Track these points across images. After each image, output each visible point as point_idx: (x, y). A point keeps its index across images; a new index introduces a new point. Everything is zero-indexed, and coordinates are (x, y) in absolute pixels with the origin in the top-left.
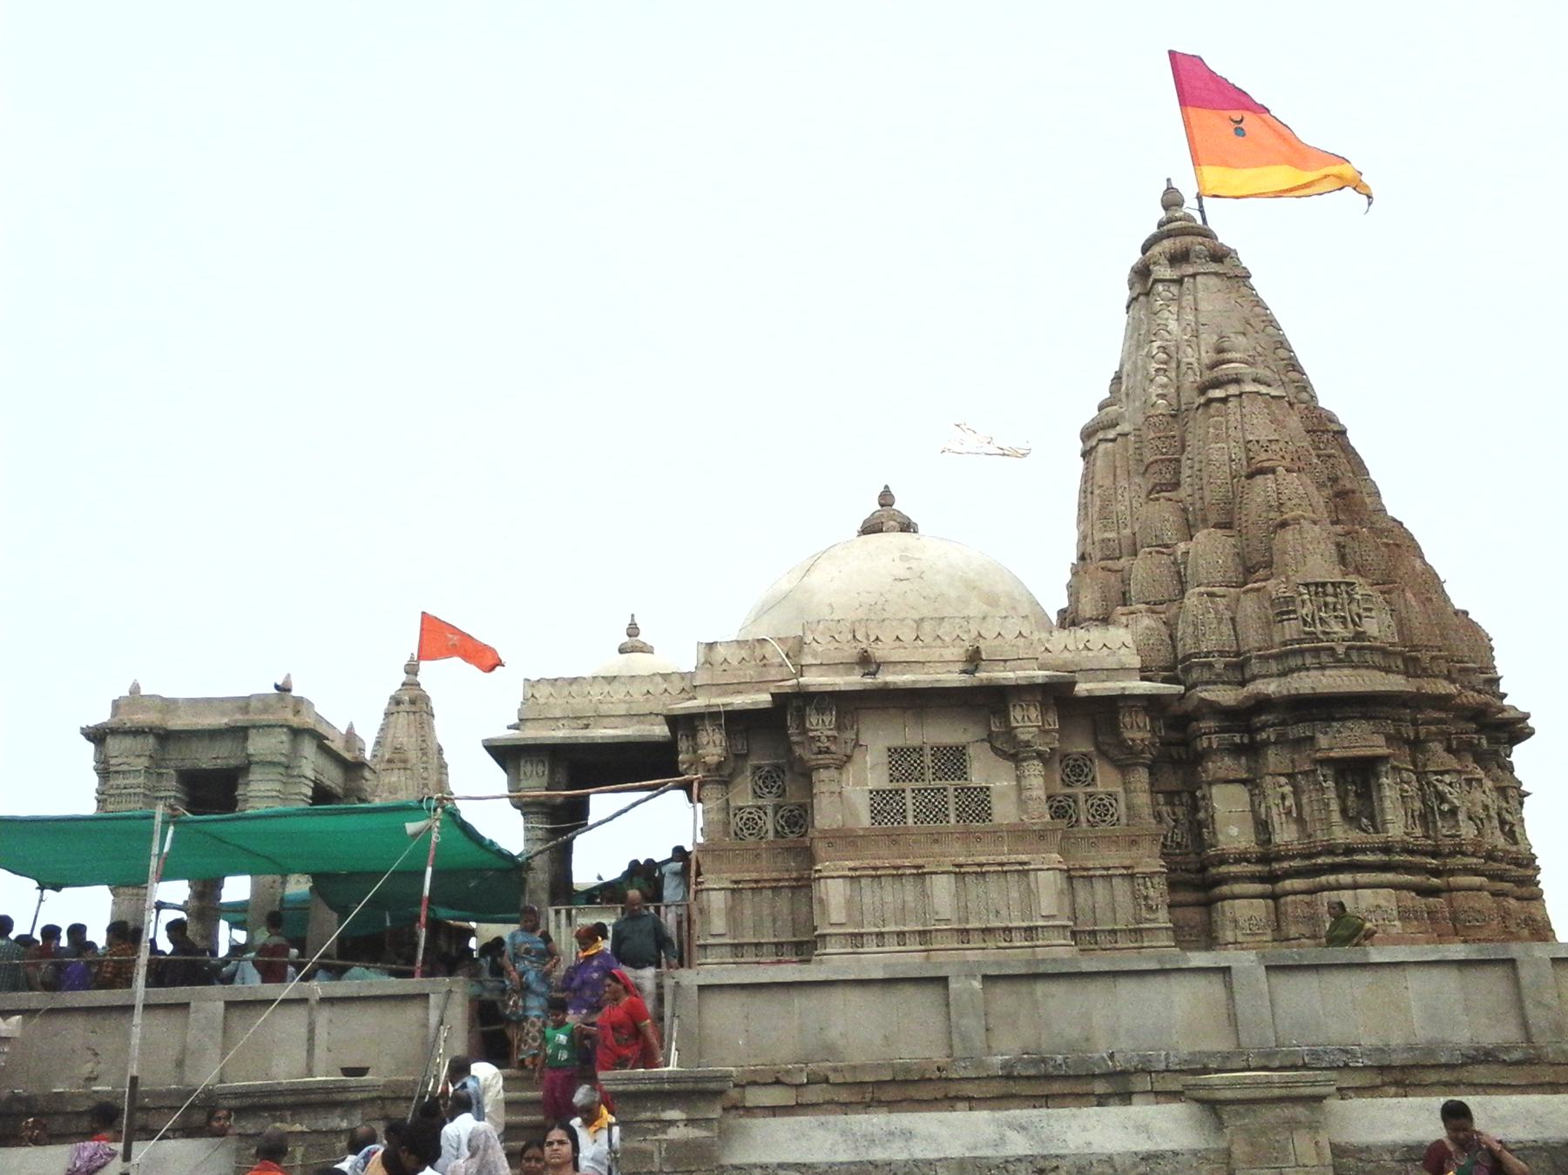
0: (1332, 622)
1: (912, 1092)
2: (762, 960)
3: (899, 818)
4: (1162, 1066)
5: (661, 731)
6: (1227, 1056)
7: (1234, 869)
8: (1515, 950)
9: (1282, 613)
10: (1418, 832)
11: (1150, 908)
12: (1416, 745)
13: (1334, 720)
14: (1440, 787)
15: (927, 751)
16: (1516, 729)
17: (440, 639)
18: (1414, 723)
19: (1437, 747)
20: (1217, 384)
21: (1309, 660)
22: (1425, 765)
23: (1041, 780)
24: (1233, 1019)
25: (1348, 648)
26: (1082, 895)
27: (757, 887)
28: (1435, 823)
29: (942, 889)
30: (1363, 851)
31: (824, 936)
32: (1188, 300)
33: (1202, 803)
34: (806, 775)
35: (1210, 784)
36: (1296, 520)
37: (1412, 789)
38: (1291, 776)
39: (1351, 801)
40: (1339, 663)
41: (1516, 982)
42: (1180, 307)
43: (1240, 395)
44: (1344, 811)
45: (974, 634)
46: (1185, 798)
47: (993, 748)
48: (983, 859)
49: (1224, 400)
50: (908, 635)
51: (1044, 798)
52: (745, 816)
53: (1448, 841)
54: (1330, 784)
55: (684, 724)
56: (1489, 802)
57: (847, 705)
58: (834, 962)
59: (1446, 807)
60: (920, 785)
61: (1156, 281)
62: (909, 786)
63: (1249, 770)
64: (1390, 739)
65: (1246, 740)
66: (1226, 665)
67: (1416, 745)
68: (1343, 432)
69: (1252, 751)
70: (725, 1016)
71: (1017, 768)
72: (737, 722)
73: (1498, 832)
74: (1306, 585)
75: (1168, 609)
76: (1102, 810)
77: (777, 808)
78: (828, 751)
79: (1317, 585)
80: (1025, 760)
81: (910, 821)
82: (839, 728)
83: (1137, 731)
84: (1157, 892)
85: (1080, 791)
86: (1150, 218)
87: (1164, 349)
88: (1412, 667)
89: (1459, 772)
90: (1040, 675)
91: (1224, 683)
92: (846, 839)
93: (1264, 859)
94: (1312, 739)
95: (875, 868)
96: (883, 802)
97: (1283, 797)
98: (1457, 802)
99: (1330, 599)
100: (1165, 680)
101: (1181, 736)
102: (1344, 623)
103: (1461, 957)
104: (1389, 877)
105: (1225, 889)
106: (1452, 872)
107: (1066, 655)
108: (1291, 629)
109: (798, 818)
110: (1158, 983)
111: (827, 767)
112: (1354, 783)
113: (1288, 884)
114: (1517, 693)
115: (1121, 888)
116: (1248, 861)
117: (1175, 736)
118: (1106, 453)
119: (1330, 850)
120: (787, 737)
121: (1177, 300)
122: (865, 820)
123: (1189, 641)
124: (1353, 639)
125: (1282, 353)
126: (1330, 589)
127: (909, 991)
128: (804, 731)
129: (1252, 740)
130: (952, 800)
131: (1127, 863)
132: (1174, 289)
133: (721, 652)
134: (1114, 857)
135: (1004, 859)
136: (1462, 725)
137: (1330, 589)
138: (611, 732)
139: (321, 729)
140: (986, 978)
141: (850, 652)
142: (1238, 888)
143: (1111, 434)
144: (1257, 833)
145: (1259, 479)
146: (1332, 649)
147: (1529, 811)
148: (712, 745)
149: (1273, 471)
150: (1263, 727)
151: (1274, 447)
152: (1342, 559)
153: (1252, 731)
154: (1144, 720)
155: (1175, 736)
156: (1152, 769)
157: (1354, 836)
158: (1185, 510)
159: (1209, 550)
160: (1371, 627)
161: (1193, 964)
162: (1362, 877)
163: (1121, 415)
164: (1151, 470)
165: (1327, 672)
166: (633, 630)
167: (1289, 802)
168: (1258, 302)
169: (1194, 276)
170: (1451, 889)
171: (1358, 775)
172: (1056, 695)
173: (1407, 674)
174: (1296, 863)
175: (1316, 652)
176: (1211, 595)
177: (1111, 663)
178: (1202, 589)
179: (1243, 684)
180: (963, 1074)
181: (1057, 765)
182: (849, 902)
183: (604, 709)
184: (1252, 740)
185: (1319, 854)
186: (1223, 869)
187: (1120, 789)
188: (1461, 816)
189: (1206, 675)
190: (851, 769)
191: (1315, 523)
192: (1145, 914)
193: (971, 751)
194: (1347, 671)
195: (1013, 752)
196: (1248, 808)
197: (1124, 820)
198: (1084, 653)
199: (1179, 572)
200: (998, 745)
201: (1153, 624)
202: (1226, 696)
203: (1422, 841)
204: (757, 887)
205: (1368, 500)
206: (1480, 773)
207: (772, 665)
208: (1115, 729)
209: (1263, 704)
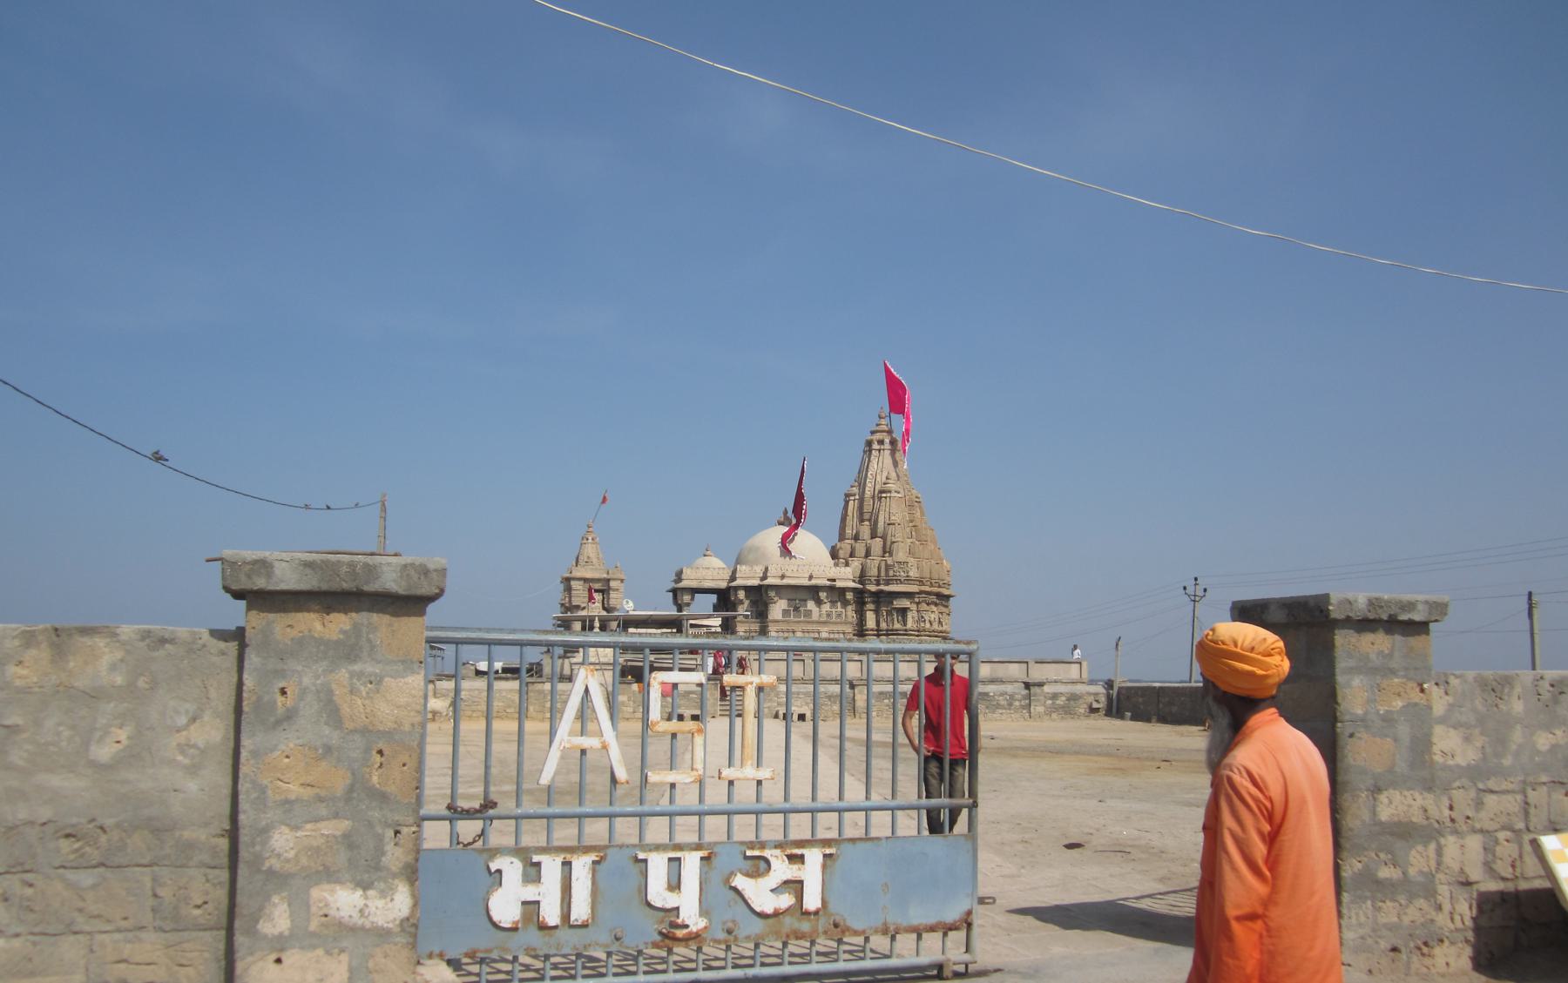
34: (766, 605)
83: (849, 596)
88: (921, 583)
96: (786, 612)
134: (840, 628)
172: (831, 589)
202: (873, 588)
209: (882, 592)
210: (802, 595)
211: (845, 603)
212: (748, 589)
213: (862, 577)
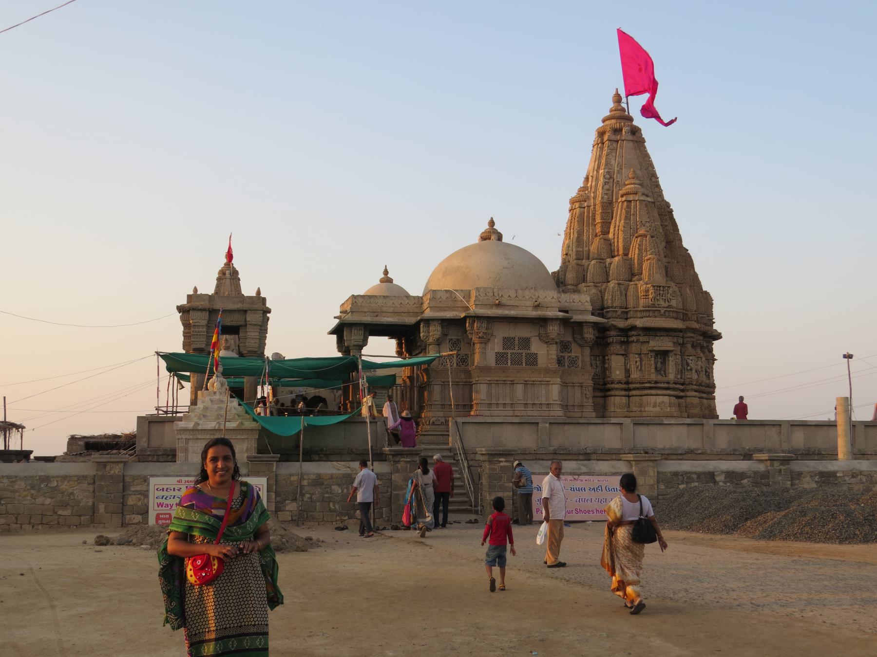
6: (619, 450)
7: (617, 386)
12: (682, 345)
16: (718, 336)
21: (651, 314)
29: (519, 389)
37: (679, 362)
38: (640, 354)
39: (659, 365)
44: (656, 368)
50: (513, 294)
62: (509, 351)
64: (674, 343)
67: (682, 345)
69: (627, 343)
77: (458, 355)
83: (589, 334)
84: (589, 392)
85: (566, 355)
88: (685, 317)
92: (485, 370)
93: (627, 383)
104: (668, 392)
105: (612, 393)
106: (688, 390)
113: (634, 393)
123: (610, 302)
127: (526, 426)
130: (524, 357)
132: (615, 145)
142: (617, 393)
147: (716, 366)
151: (648, 224)
154: (591, 330)
156: (592, 348)
157: (659, 378)
158: (611, 245)
160: (674, 303)
162: (659, 392)
166: (386, 272)
167: (638, 364)
168: (647, 156)
173: (684, 320)
174: (638, 386)
177: (582, 308)
179: (627, 319)
183: (384, 309)
186: (613, 386)
187: (579, 355)
190: (490, 345)
192: (585, 400)
193: (532, 340)
195: (546, 341)
202: (621, 324)
206: (702, 355)
208: (581, 333)
209: (633, 328)
210: (521, 332)
212: (446, 323)
213: (600, 310)
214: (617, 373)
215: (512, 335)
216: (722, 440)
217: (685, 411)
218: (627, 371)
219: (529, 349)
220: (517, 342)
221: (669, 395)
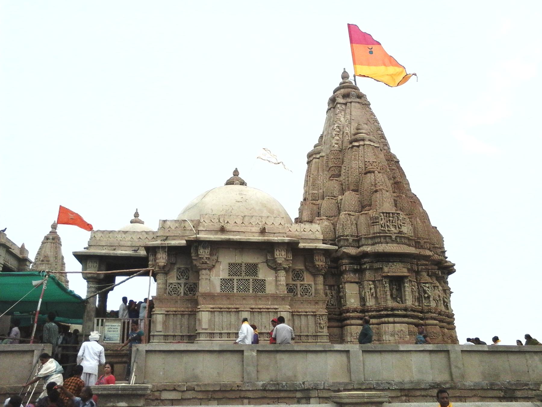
0: (391, 227)
1: (227, 395)
2: (167, 341)
3: (231, 290)
4: (322, 387)
5: (142, 253)
6: (346, 384)
7: (351, 314)
8: (449, 347)
9: (374, 223)
10: (417, 304)
11: (321, 328)
12: (418, 273)
13: (390, 262)
14: (425, 288)
15: (243, 265)
16: (449, 269)
17: (67, 217)
18: (417, 265)
19: (425, 274)
20: (356, 140)
21: (382, 240)
22: (420, 280)
23: (284, 278)
24: (349, 371)
25: (396, 236)
26: (297, 322)
27: (175, 314)
28: (422, 301)
30: (398, 310)
31: (199, 333)
32: (348, 111)
33: (341, 290)
34: (197, 272)
35: (345, 283)
36: (381, 190)
37: (415, 289)
38: (374, 282)
40: (393, 242)
41: (449, 358)
42: (345, 113)
43: (364, 145)
44: (392, 295)
45: (264, 223)
46: (336, 287)
47: (268, 266)
48: (261, 306)
49: (358, 146)
50: (239, 221)
51: (285, 284)
52: (173, 286)
53: (426, 308)
54: (387, 285)
55: (152, 250)
56: (440, 295)
57: (215, 246)
58: (202, 343)
59: (426, 295)
60: (240, 278)
61: (337, 103)
62: (235, 278)
63: (359, 279)
64: (409, 270)
65: (358, 268)
66: (353, 240)
67: (418, 273)
68: (398, 162)
69: (360, 272)
70: (155, 362)
71: (276, 273)
72: (172, 251)
73: (442, 305)
74: (383, 213)
75: (334, 219)
76: (306, 290)
77: (185, 284)
78: (206, 263)
79: (387, 213)
80: (279, 270)
81: (235, 291)
82: (211, 255)
83: (320, 262)
84: (324, 321)
85: (298, 283)
86: (337, 81)
87: (338, 127)
88: (417, 245)
89: (431, 283)
90: (287, 239)
91: (352, 246)
92: (210, 297)
94: (382, 268)
95: (221, 308)
97: (371, 289)
98: (430, 294)
99: (391, 219)
100: (331, 244)
101: (335, 265)
102: (396, 228)
103: (431, 349)
104: (406, 320)
106: (427, 319)
107: (297, 232)
108: (377, 228)
109: (193, 288)
110: (323, 355)
111: (205, 269)
112: (396, 285)
114: (451, 257)
115: (311, 319)
116: (357, 312)
117: (334, 265)
118: (316, 162)
119: (386, 309)
120: (191, 257)
121: (344, 110)
122: (218, 290)
123: (341, 231)
124: (398, 233)
125: (379, 132)
126: (391, 215)
127: (228, 355)
128: (198, 255)
129: (361, 267)
130: (251, 284)
131: (314, 310)
132: (344, 106)
133: (168, 223)
134: (310, 308)
135: (269, 307)
136: (433, 267)
137: (391, 215)
138: (124, 252)
139: (8, 244)
140: (258, 351)
141: (217, 226)
142: (353, 322)
143: (318, 156)
144: (361, 302)
145: (369, 175)
146: (391, 236)
147: (453, 298)
148: (162, 259)
149: (374, 172)
150: (365, 264)
151: (374, 164)
152: (396, 205)
153: (361, 264)
155: (334, 265)
157: (394, 304)
158: (342, 184)
159: (350, 199)
160: (405, 229)
161: (335, 349)
162: (397, 319)
163: (322, 150)
164: (332, 169)
165: (389, 245)
166: (136, 215)
168: (372, 114)
169: (351, 102)
170: (426, 325)
171: (397, 282)
172: (292, 247)
173: (416, 247)
175: (386, 237)
176: (349, 214)
177: (312, 237)
178: (346, 212)
179: (358, 247)
180: (247, 388)
181: (291, 273)
182: (210, 321)
183: (122, 243)
184: (361, 267)
185: (382, 310)
186: (348, 314)
187: (313, 283)
188: (431, 299)
189: (346, 243)
190: (214, 271)
191: (387, 191)
192: (319, 330)
193: (259, 266)
194: (395, 245)
195: (275, 267)
196: (358, 292)
197: (313, 295)
198: (303, 233)
199: (338, 206)
200: (270, 264)
201: (328, 224)
202: (352, 251)
203: (417, 307)
204: (175, 314)
205: (405, 186)
207: (188, 230)
208: (312, 262)
209: (365, 255)
210: (249, 259)
211: (315, 272)
214: (352, 301)
215: (239, 261)
216: (474, 372)
217: (424, 337)
218: (363, 300)
219: (256, 275)
220: (243, 268)
221: (408, 323)
